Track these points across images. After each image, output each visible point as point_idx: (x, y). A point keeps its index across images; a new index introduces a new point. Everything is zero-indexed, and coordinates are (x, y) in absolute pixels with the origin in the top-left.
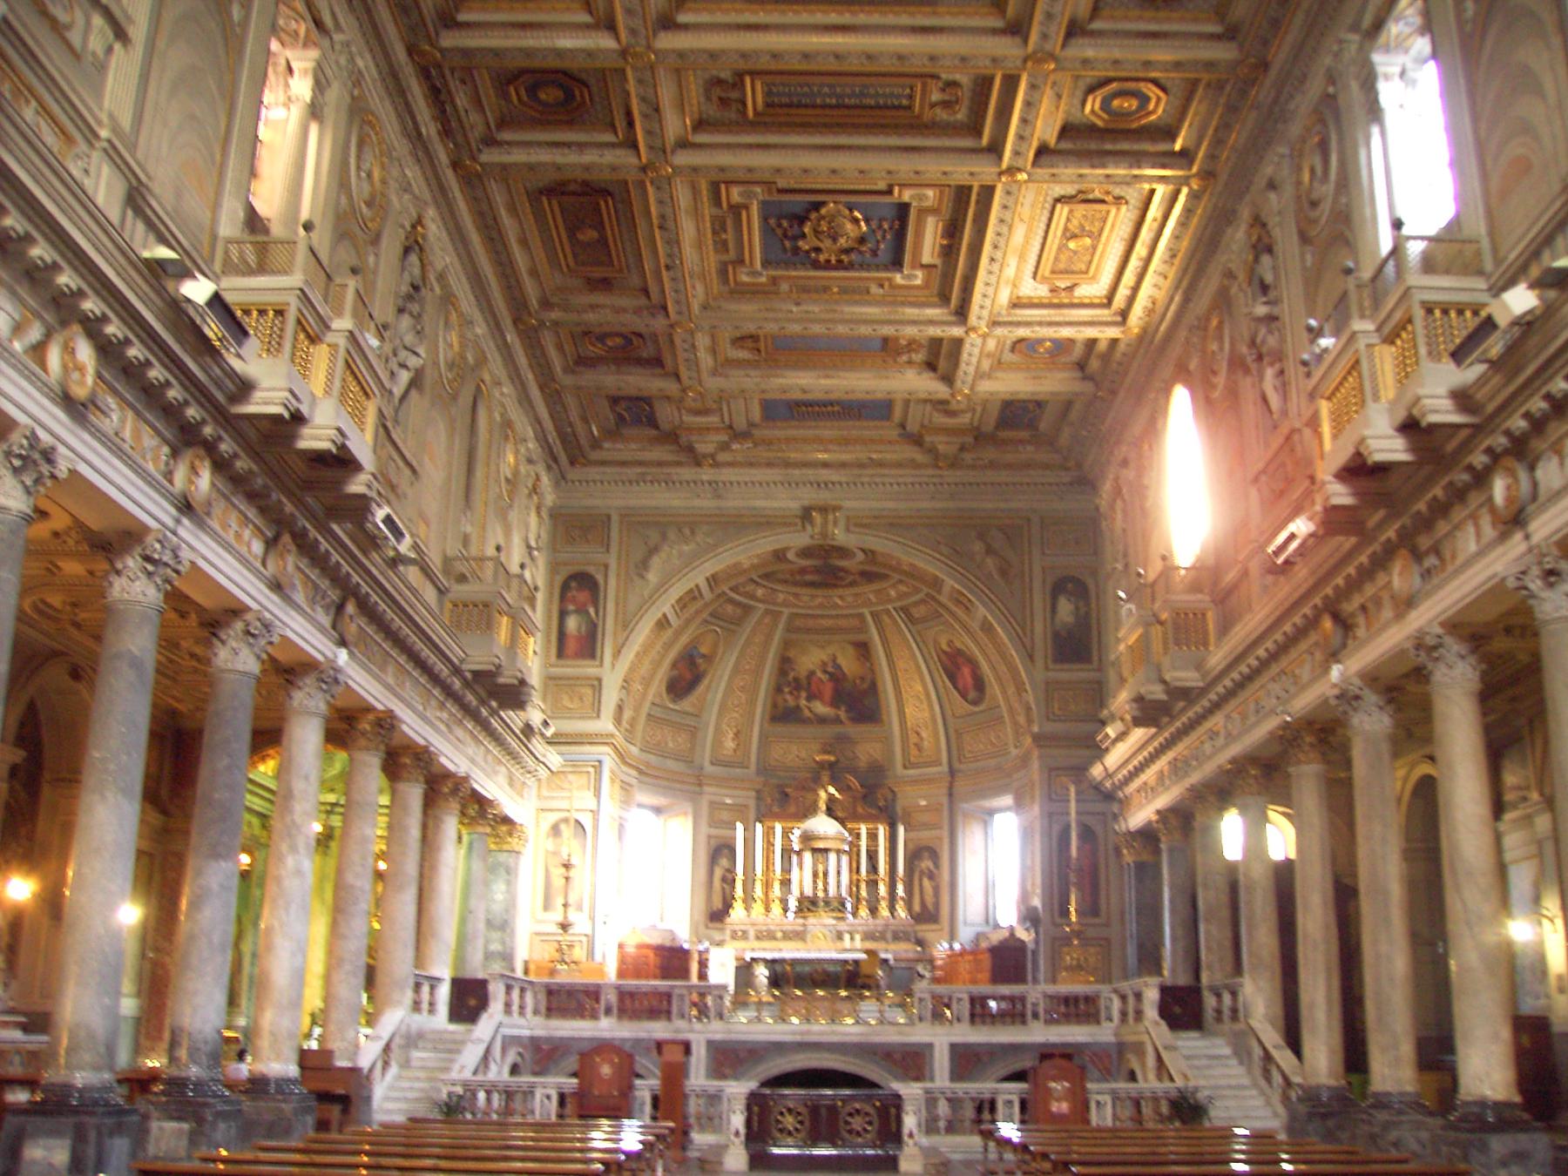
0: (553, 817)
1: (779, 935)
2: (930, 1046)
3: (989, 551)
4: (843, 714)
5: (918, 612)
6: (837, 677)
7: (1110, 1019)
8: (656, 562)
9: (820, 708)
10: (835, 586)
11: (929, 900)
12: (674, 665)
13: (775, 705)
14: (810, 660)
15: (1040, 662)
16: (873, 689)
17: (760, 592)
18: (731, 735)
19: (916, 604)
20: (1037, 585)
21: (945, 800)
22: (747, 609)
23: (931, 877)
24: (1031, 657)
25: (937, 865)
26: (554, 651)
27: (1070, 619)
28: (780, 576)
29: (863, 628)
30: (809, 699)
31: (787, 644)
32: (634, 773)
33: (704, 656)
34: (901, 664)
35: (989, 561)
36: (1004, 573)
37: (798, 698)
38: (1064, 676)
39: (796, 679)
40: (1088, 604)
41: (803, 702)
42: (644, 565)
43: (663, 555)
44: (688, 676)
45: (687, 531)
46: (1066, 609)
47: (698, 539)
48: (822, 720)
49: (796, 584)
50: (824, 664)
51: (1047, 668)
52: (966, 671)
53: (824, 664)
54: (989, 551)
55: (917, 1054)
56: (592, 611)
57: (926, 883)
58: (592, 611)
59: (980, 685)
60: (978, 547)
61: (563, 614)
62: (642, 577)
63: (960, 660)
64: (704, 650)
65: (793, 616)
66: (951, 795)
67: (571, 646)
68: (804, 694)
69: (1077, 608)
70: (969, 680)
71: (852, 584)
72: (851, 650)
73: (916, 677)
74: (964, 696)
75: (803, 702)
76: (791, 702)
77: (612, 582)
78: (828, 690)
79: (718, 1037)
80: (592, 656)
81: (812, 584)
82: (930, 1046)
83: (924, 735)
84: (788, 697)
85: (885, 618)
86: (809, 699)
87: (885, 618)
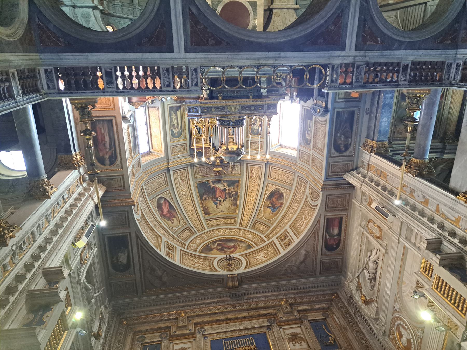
0: (347, 153)
1: (253, 108)
2: (186, 51)
3: (160, 278)
4: (212, 184)
5: (187, 233)
6: (215, 199)
7: (46, 71)
8: (302, 258)
9: (220, 186)
10: (220, 240)
11: (174, 116)
12: (281, 205)
13: (238, 186)
14: (226, 205)
15: (133, 235)
16: (201, 198)
17: (250, 237)
18: (254, 175)
19: (188, 237)
20: (137, 268)
21: (170, 157)
22: (253, 226)
23: (174, 125)
24: (137, 237)
25: (172, 130)
26: (344, 220)
27: (120, 254)
28: (244, 245)
29: (208, 220)
30: (225, 190)
31: (235, 211)
32: (298, 164)
33: (269, 207)
34: (191, 208)
35: (160, 273)
36: (153, 270)
37: (229, 190)
38: (121, 231)
39: (230, 197)
40: (112, 262)
41: (227, 188)
42: (306, 256)
43: (299, 261)
44: (274, 199)
45: (289, 271)
46: (123, 258)
47: (284, 269)
48: (219, 182)
49: (236, 240)
50: (220, 204)
51: (130, 233)
52: (165, 211)
53: (220, 204)
54: (160, 278)
55: (197, 44)
56: (328, 237)
57: (176, 124)
58: (328, 237)
59: (159, 206)
60: (165, 279)
61: (339, 234)
62: (307, 252)
63: (168, 215)
64: (269, 210)
65: (234, 224)
66: (168, 160)
67: (336, 223)
68: (227, 191)
69: (117, 259)
70: (164, 207)
71: (214, 242)
72: (211, 210)
73: (186, 204)
74: (165, 199)
75: (227, 188)
76: (231, 188)
77: (319, 249)
78: (218, 194)
79: (337, 53)
80: (328, 219)
81: (230, 240)
82: (186, 51)
83: (180, 181)
84: (233, 190)
85: (200, 229)
86: (225, 190)
87: (200, 228)
